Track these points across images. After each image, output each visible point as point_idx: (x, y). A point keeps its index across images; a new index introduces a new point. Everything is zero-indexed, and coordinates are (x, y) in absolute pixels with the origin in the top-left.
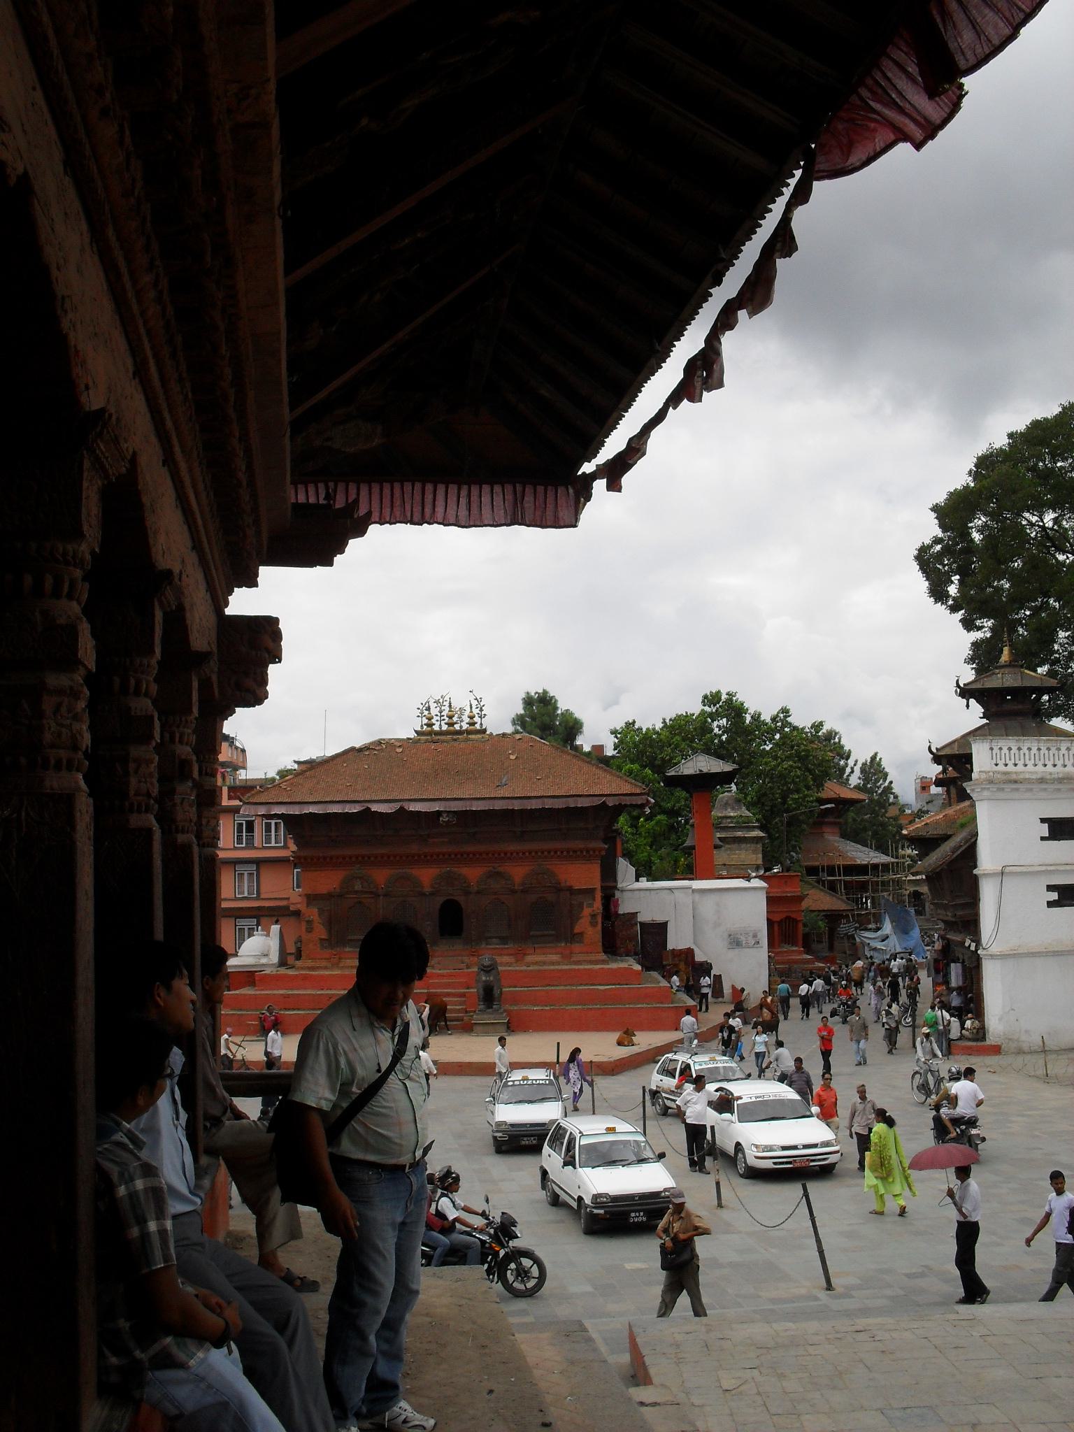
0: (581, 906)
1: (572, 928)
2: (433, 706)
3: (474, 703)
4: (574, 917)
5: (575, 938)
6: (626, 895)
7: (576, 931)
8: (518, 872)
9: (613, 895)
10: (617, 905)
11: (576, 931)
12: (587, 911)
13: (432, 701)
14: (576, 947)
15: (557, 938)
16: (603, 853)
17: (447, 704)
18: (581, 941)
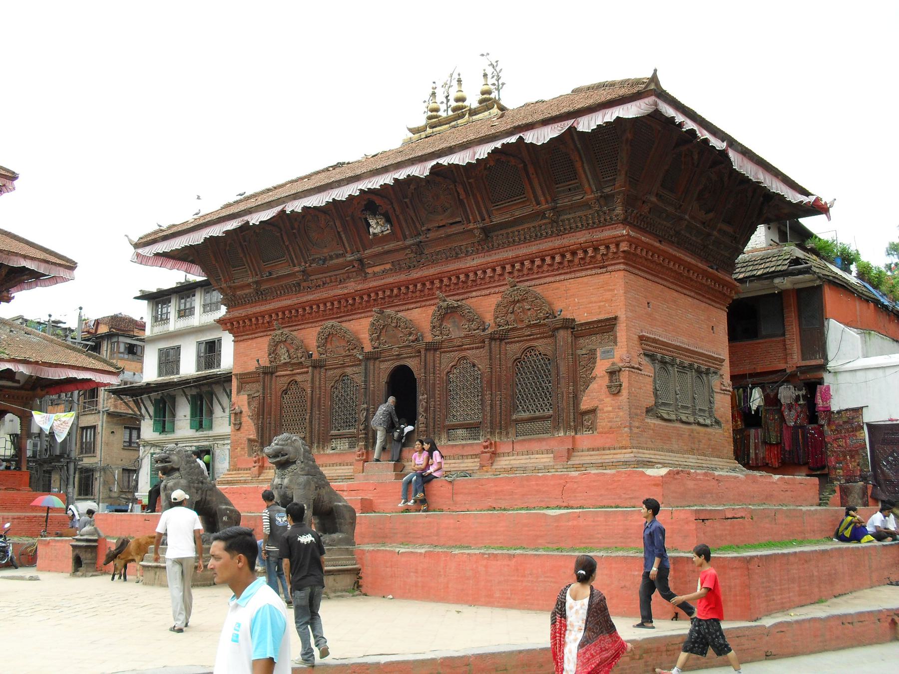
0: (592, 356)
1: (576, 399)
3: (489, 71)
4: (579, 380)
5: (581, 419)
6: (841, 378)
7: (584, 406)
8: (486, 305)
9: (820, 381)
10: (827, 396)
11: (584, 406)
12: (601, 367)
13: (439, 85)
14: (585, 439)
15: (556, 422)
16: (624, 247)
17: (455, 83)
18: (592, 428)
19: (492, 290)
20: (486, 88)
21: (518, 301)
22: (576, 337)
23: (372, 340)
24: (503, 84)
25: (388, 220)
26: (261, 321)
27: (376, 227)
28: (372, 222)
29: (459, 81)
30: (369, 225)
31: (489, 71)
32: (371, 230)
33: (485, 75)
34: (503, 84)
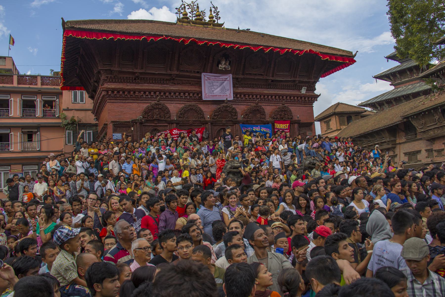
2: (187, 7)
3: (213, 9)
17: (195, 7)
19: (268, 104)
20: (211, 16)
21: (283, 111)
22: (300, 127)
23: (215, 116)
24: (220, 18)
25: (229, 64)
26: (137, 93)
27: (222, 66)
28: (224, 62)
29: (198, 7)
30: (219, 63)
31: (213, 9)
32: (220, 66)
33: (211, 10)
34: (220, 18)
